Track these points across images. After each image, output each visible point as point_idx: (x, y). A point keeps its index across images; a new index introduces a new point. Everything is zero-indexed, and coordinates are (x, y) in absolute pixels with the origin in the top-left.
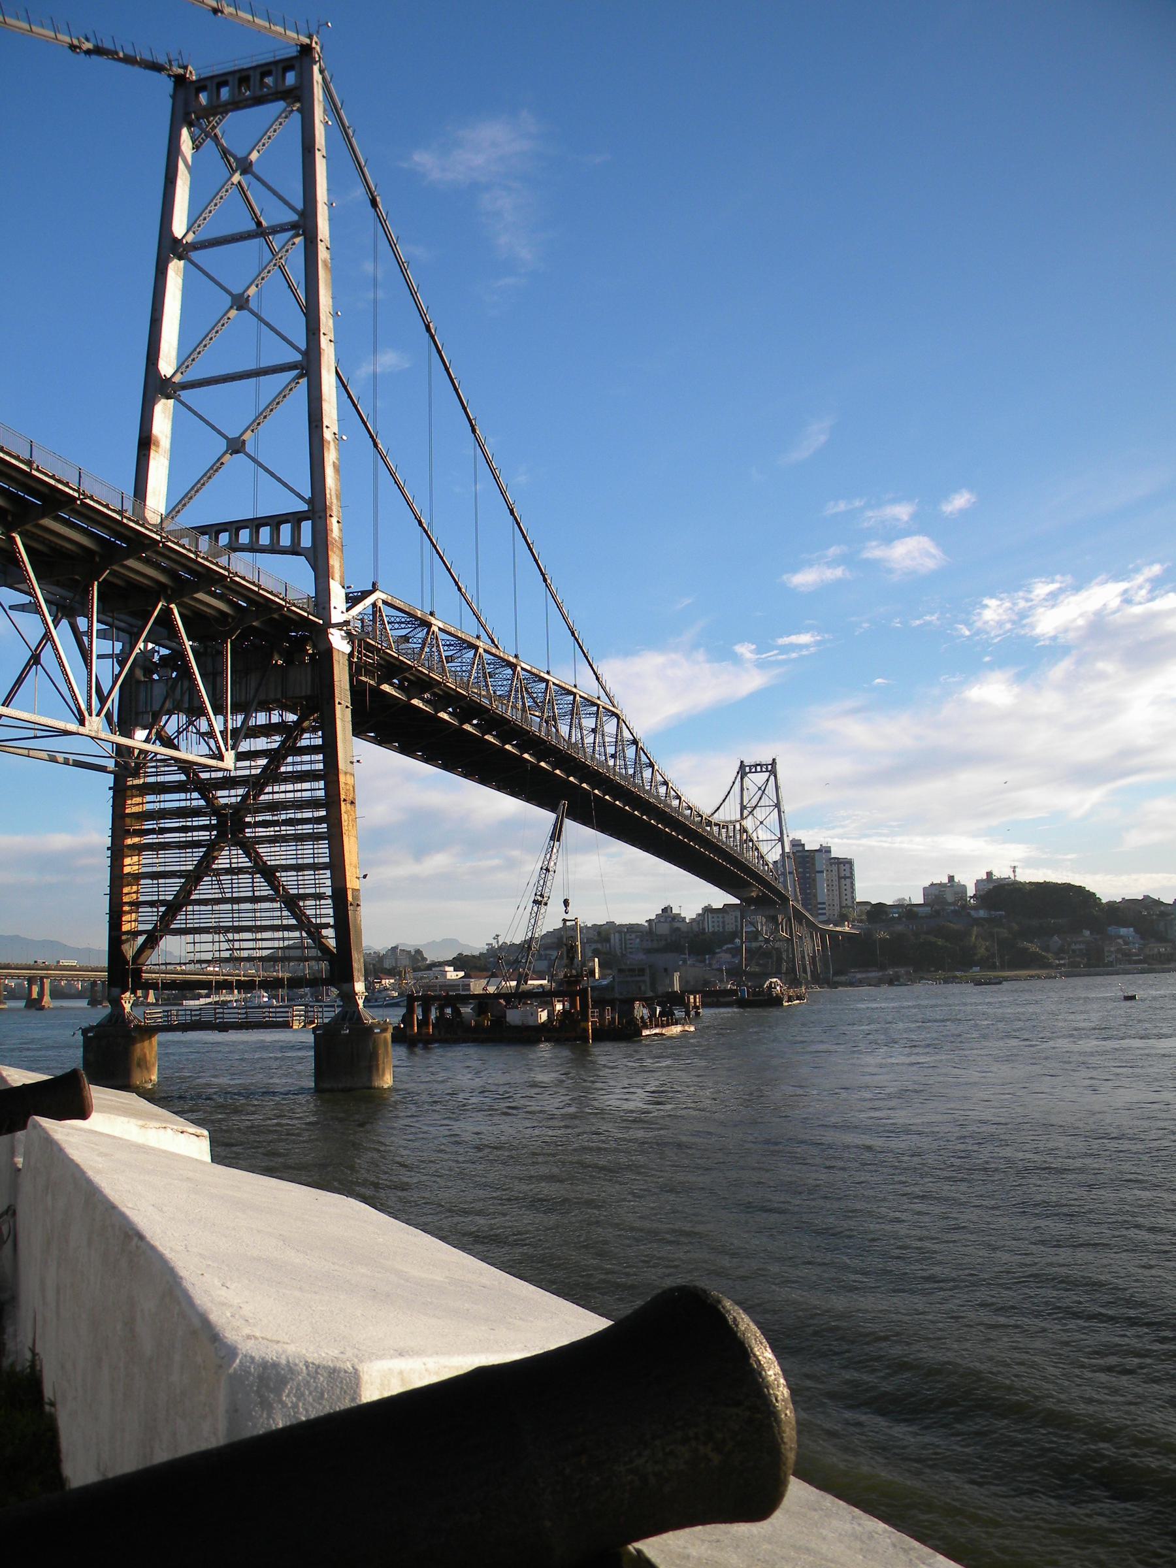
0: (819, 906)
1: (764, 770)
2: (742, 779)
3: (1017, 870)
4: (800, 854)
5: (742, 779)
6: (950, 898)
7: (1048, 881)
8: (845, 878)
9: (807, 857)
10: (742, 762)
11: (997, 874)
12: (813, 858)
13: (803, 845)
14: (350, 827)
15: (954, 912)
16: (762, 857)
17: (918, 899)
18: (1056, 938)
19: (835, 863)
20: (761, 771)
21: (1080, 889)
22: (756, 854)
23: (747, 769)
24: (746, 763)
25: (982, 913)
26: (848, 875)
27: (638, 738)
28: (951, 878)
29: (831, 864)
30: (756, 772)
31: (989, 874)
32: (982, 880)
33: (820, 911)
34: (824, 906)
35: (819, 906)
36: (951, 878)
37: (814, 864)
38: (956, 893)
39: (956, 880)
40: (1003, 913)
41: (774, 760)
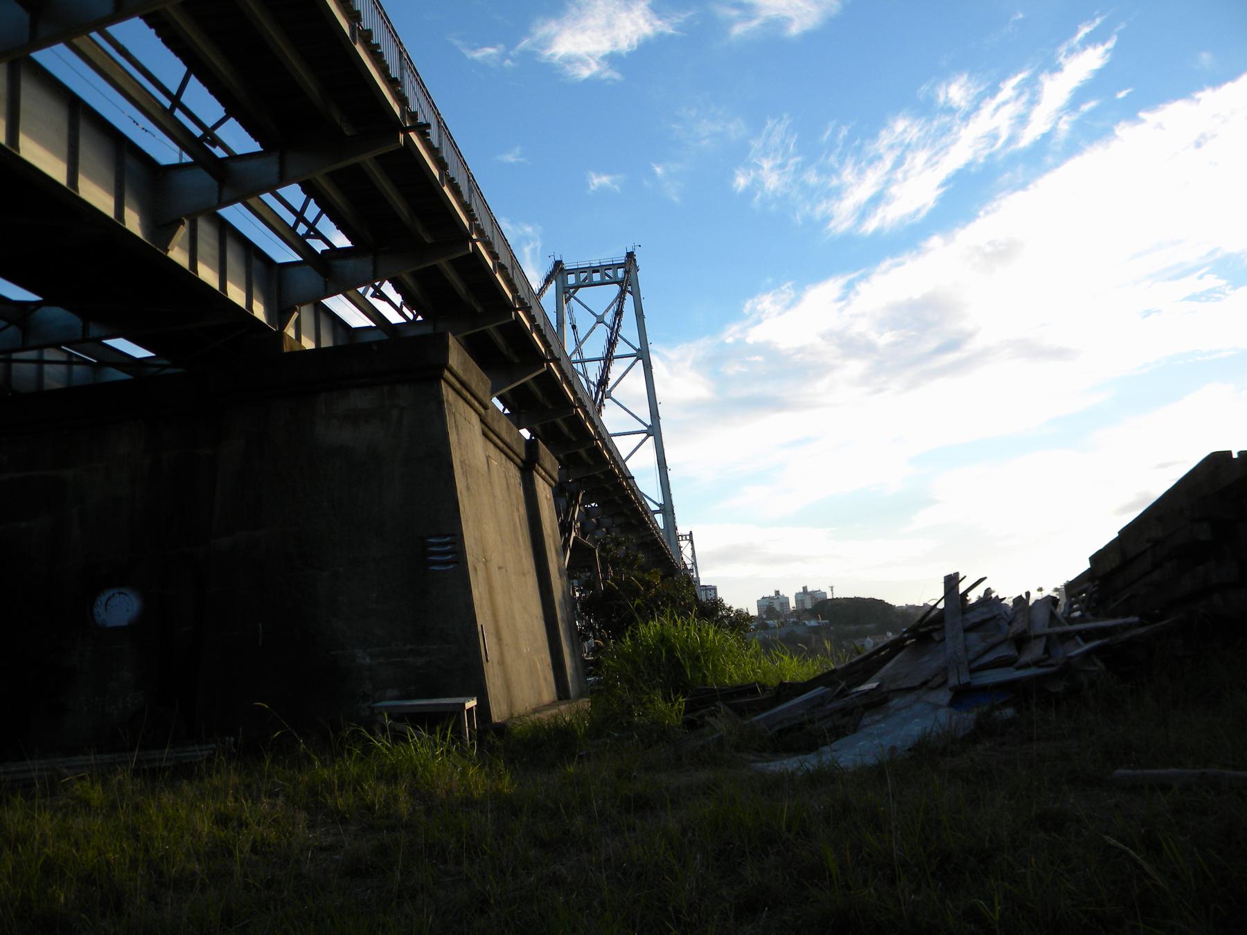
1: (684, 539)
3: (834, 589)
6: (778, 609)
7: (857, 596)
11: (809, 590)
15: (794, 622)
17: (754, 612)
18: (868, 639)
21: (881, 602)
25: (813, 623)
28: (777, 593)
31: (805, 588)
32: (800, 593)
36: (777, 593)
38: (782, 604)
39: (781, 594)
40: (827, 621)
41: (691, 533)
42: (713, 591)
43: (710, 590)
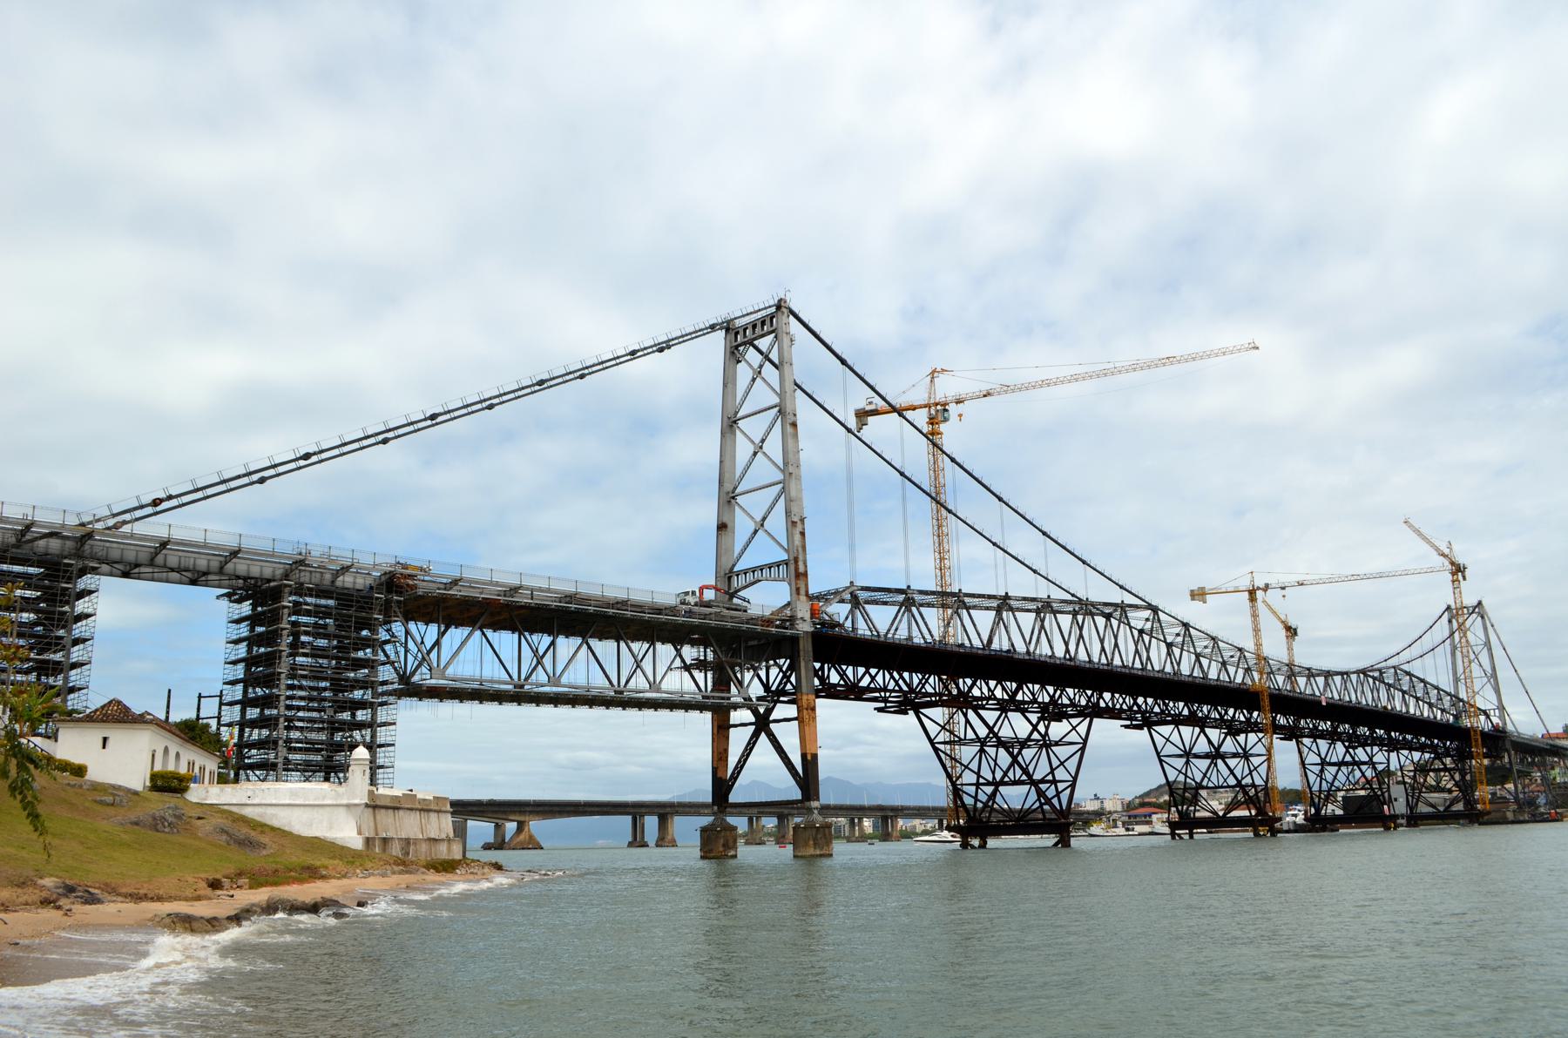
14: (811, 722)
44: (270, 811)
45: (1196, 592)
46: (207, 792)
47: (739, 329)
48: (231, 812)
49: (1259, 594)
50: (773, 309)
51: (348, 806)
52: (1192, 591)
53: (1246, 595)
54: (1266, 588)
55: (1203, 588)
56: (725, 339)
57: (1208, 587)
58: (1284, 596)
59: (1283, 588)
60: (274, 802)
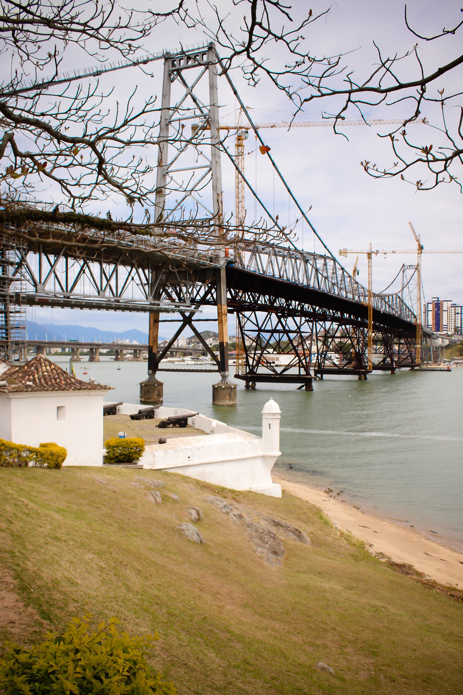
0: (444, 327)
2: (403, 272)
4: (435, 302)
5: (403, 272)
8: (458, 313)
9: (440, 303)
10: (403, 265)
12: (442, 305)
13: (438, 298)
16: (408, 308)
19: (454, 307)
20: (412, 269)
22: (404, 306)
23: (406, 267)
24: (405, 265)
26: (459, 312)
27: (343, 267)
29: (452, 307)
30: (410, 269)
33: (444, 329)
34: (446, 327)
35: (444, 327)
37: (442, 307)
42: (460, 308)
43: (458, 307)
44: (207, 469)
45: (342, 251)
46: (154, 456)
47: (176, 59)
48: (176, 475)
49: (373, 255)
50: (206, 49)
51: (263, 457)
52: (340, 250)
53: (366, 255)
54: (377, 252)
55: (346, 249)
56: (165, 64)
57: (349, 249)
58: (385, 258)
59: (385, 254)
60: (211, 460)
